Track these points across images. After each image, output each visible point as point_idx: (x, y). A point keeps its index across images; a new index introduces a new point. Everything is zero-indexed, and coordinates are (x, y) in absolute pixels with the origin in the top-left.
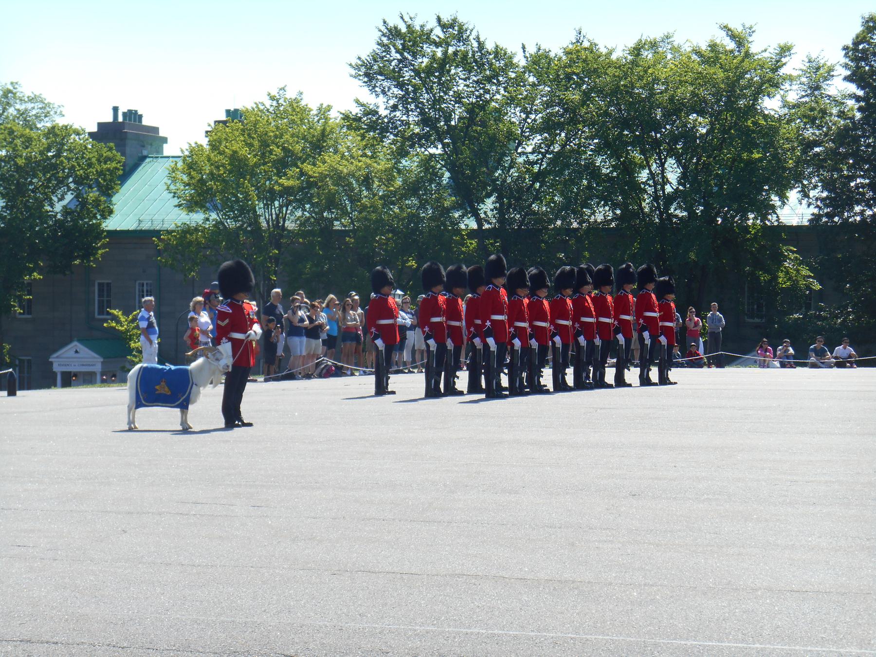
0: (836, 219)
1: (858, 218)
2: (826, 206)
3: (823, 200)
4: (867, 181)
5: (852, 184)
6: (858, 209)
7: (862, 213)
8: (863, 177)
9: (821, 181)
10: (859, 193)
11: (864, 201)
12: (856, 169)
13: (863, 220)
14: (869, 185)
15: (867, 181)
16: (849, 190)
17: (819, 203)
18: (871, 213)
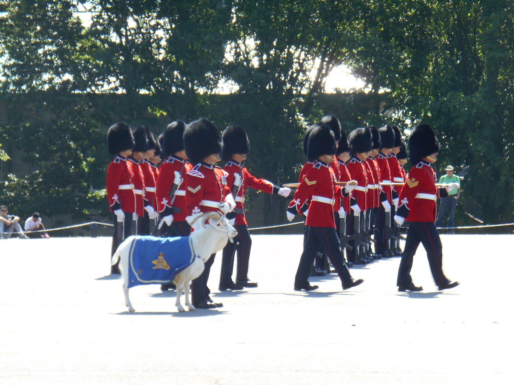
0: (24, 87)
1: (46, 87)
2: (14, 74)
3: (9, 67)
4: (54, 48)
5: (40, 51)
6: (46, 77)
7: (51, 80)
8: (51, 44)
9: (8, 47)
10: (47, 61)
11: (53, 69)
12: (43, 35)
13: (52, 88)
14: (56, 52)
15: (54, 48)
16: (37, 58)
17: (6, 71)
18: (60, 81)
